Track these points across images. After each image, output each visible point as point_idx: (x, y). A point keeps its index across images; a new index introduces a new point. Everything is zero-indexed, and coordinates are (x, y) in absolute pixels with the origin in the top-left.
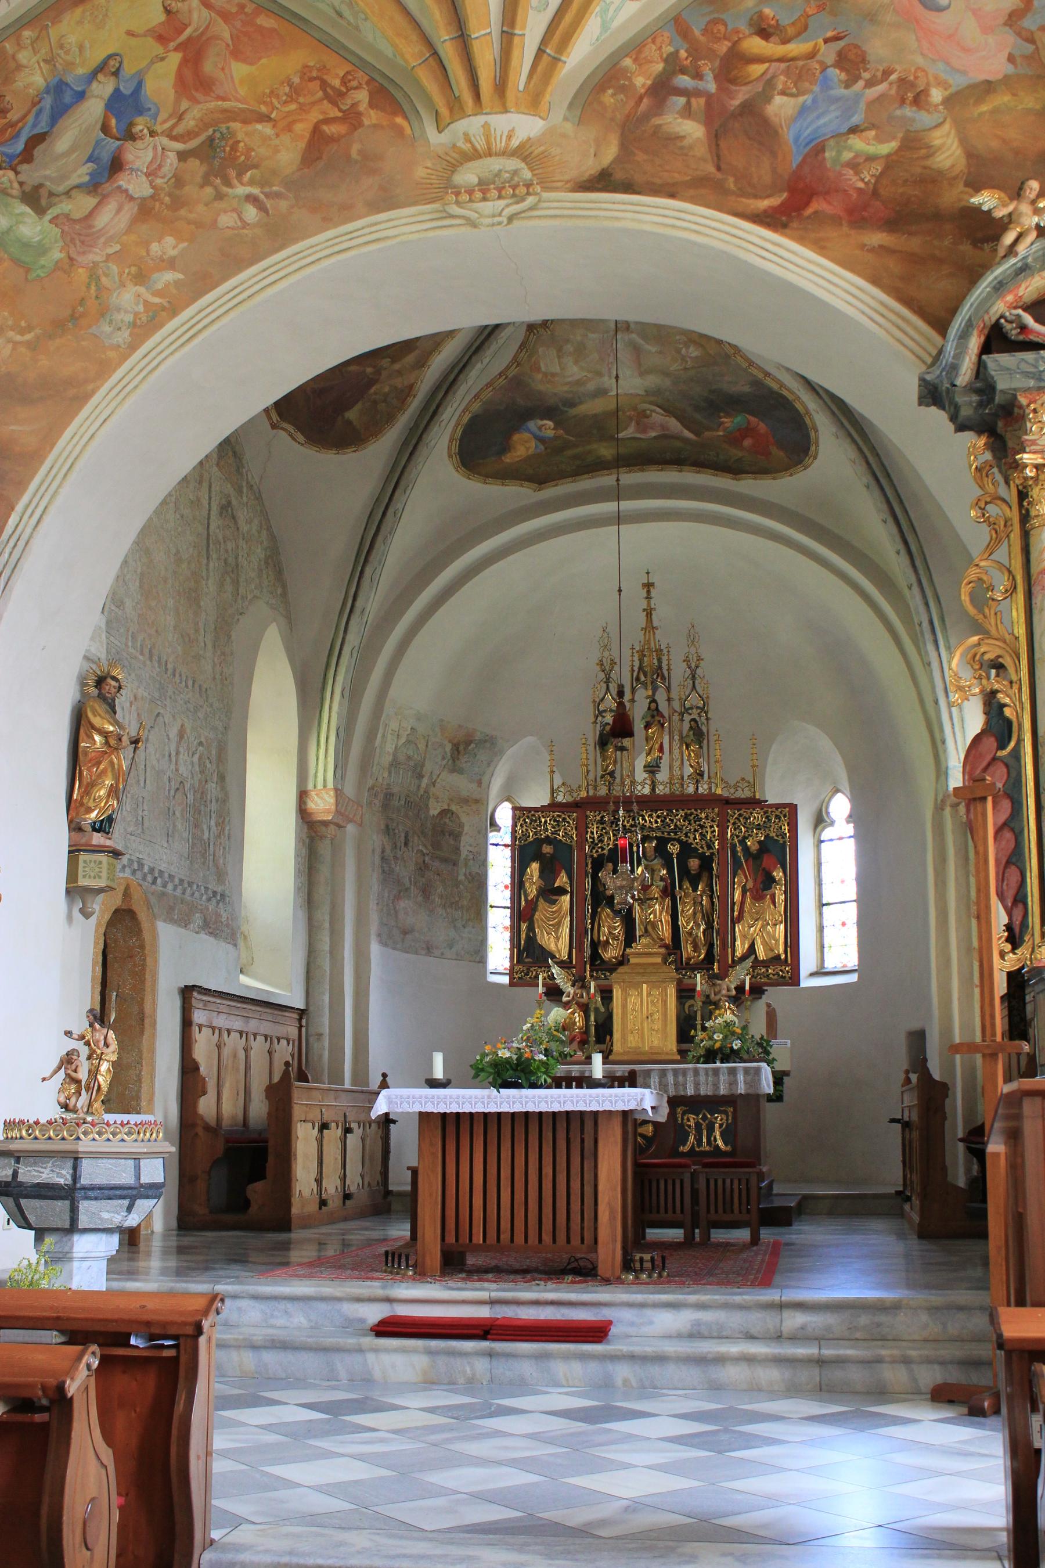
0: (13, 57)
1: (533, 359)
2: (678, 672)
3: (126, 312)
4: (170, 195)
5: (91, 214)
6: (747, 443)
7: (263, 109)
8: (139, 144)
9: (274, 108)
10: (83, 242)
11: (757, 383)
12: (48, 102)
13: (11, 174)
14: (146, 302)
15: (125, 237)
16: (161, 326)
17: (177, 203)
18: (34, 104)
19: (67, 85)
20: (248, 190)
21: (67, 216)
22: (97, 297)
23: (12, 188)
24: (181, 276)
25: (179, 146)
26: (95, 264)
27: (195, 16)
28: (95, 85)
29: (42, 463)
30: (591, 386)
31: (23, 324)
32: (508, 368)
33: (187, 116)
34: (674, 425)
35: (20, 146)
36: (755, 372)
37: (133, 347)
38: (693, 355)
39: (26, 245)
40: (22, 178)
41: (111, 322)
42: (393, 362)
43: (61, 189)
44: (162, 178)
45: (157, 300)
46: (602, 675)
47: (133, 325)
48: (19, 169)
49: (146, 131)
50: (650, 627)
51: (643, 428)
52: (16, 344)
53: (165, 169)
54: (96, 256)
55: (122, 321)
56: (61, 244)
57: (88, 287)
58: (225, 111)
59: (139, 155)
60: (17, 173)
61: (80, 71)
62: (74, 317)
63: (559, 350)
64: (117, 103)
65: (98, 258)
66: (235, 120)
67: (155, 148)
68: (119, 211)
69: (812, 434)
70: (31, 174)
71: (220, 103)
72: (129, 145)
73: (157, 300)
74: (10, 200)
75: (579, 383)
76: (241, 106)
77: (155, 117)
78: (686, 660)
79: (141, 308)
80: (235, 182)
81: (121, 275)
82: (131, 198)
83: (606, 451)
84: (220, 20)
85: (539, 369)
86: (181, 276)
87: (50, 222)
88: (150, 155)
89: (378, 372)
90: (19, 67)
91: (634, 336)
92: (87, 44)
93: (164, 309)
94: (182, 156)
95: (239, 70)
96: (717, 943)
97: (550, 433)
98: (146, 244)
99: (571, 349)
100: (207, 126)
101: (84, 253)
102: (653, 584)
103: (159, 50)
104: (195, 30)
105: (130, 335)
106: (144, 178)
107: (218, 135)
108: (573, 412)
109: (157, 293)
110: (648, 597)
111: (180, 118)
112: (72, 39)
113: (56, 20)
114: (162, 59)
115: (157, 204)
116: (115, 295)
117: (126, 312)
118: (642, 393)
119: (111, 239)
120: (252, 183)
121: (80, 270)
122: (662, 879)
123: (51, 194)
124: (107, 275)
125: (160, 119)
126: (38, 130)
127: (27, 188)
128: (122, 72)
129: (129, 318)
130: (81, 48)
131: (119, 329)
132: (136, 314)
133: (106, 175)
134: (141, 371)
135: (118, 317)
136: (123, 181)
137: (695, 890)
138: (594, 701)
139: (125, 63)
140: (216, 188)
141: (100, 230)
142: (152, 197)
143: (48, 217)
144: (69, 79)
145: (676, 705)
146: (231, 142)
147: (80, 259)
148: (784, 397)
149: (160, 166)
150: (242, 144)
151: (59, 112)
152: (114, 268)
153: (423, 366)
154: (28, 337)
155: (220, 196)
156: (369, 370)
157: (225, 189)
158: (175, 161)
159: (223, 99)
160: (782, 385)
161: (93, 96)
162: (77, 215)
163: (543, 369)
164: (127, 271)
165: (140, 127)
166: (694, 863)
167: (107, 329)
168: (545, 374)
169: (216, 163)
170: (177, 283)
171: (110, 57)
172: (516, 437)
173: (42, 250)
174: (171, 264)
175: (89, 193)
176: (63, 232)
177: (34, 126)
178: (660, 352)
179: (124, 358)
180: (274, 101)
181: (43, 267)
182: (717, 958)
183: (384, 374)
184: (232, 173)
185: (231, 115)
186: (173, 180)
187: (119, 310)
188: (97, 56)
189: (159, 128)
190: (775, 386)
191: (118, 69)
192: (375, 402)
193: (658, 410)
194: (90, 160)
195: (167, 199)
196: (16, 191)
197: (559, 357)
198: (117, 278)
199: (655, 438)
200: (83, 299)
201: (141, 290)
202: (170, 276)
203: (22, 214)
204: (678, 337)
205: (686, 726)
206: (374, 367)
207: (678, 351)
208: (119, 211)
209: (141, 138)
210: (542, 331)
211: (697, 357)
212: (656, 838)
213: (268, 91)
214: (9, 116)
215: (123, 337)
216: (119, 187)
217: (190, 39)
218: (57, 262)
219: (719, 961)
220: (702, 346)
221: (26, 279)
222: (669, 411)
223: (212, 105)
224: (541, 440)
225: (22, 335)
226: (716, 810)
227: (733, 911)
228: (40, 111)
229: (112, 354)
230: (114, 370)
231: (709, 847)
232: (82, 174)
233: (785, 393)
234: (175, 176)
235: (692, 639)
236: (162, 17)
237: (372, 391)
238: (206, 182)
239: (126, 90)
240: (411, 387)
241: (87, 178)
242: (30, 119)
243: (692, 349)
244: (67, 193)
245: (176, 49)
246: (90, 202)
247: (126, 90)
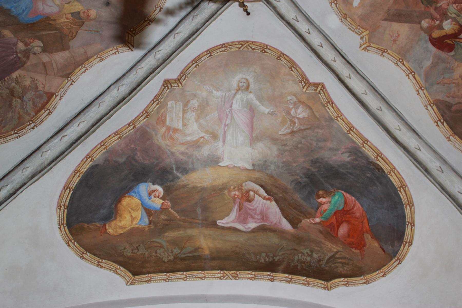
1: (162, 111)
6: (343, 230)
11: (356, 152)
30: (205, 151)
32: (138, 118)
34: (273, 209)
36: (354, 137)
38: (301, 116)
42: (44, 50)
51: (244, 216)
63: (186, 105)
69: (407, 210)
75: (197, 145)
83: (205, 242)
85: (164, 122)
89: (27, 53)
91: (252, 96)
97: (157, 203)
99: (196, 105)
108: (184, 179)
118: (250, 167)
148: (380, 169)
153: (67, 76)
156: (21, 46)
160: (379, 154)
163: (168, 123)
168: (169, 129)
172: (126, 201)
178: (272, 114)
183: (33, 60)
190: (372, 155)
192: (12, 92)
193: (262, 191)
197: (184, 112)
199: (254, 231)
204: (289, 98)
206: (26, 44)
207: (288, 113)
210: (175, 85)
211: (304, 118)
220: (310, 108)
224: (148, 211)
233: (382, 164)
237: (15, 75)
240: (50, 96)
243: (300, 110)
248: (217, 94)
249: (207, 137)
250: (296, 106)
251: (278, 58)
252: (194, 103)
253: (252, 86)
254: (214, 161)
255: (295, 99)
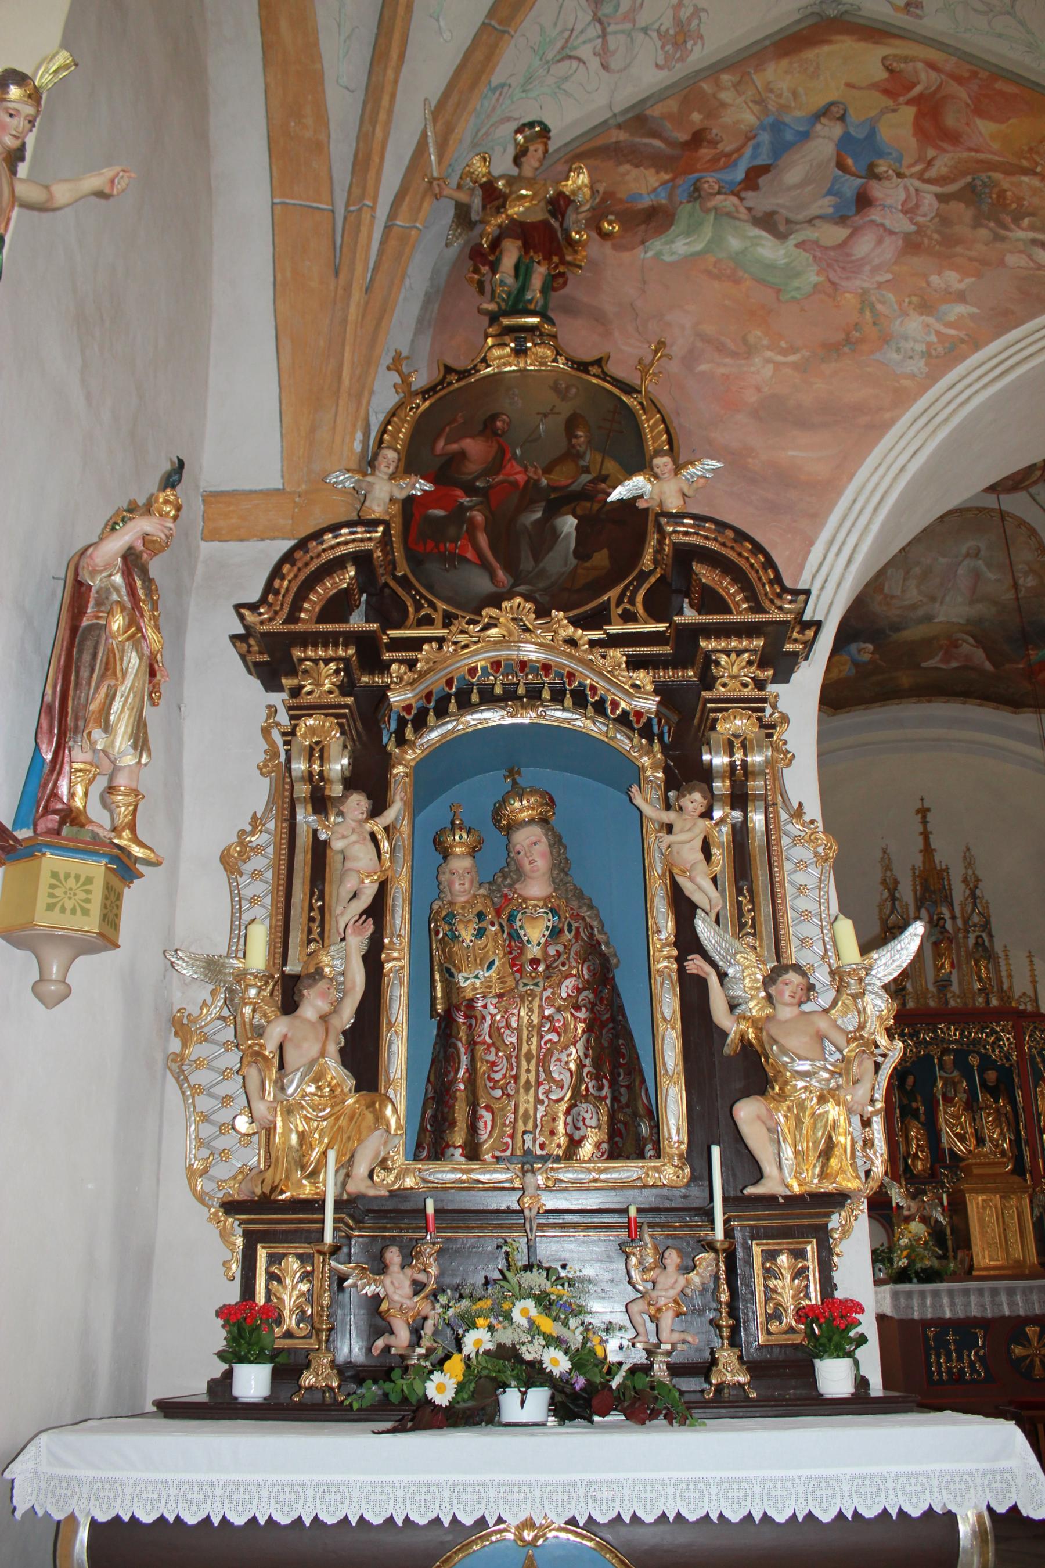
0: (714, 95)
2: (959, 892)
3: (915, 341)
4: (938, 232)
5: (845, 243)
7: (1025, 163)
8: (886, 183)
9: (1037, 164)
10: (843, 268)
12: (765, 137)
13: (735, 200)
14: (938, 333)
15: (896, 268)
16: (964, 358)
17: (950, 241)
18: (749, 139)
19: (785, 124)
20: (1031, 235)
21: (816, 242)
22: (875, 323)
23: (737, 211)
24: (975, 310)
25: (937, 189)
26: (865, 292)
27: (923, 76)
28: (818, 127)
29: (840, 494)
31: (783, 344)
33: (938, 163)
35: (740, 174)
37: (933, 378)
39: (771, 267)
40: (749, 203)
41: (898, 350)
43: (800, 217)
44: (924, 216)
45: (952, 332)
46: (886, 893)
47: (927, 354)
48: (743, 194)
49: (890, 172)
50: (928, 850)
51: (948, 657)
52: (777, 365)
53: (925, 208)
54: (864, 281)
55: (913, 350)
56: (815, 268)
57: (861, 311)
58: (981, 161)
59: (890, 194)
60: (741, 199)
61: (798, 114)
62: (848, 340)
63: (907, 573)
64: (845, 143)
65: (866, 285)
66: (995, 171)
67: (906, 188)
68: (880, 241)
70: (760, 201)
71: (973, 154)
72: (874, 184)
73: (952, 332)
74: (737, 223)
75: (914, 607)
76: (997, 158)
77: (899, 160)
78: (965, 881)
79: (934, 338)
80: (1012, 226)
81: (900, 303)
82: (891, 233)
83: (905, 680)
84: (952, 82)
86: (975, 310)
87: (797, 246)
88: (902, 196)
90: (723, 105)
92: (801, 90)
93: (962, 341)
94: (941, 198)
95: (985, 127)
96: (1027, 1154)
98: (925, 276)
100: (964, 174)
101: (848, 279)
102: (928, 810)
103: (890, 103)
104: (926, 88)
105: (926, 364)
106: (901, 215)
107: (979, 183)
108: (895, 636)
109: (949, 325)
110: (924, 822)
111: (930, 163)
112: (784, 85)
113: (759, 67)
114: (894, 111)
115: (926, 241)
116: (898, 322)
117: (915, 341)
118: (961, 621)
119: (875, 270)
120: (1032, 228)
121: (847, 295)
122: (965, 1091)
123: (788, 221)
124: (883, 303)
125: (905, 163)
126: (759, 162)
127: (759, 215)
128: (848, 119)
129: (921, 347)
130: (795, 94)
131: (911, 358)
132: (929, 344)
133: (854, 209)
134: (949, 403)
135: (909, 345)
136: (875, 215)
137: (997, 1102)
138: (881, 918)
139: (851, 112)
140: (991, 230)
141: (862, 259)
142: (917, 232)
143: (792, 241)
144: (787, 119)
145: (960, 922)
146: (996, 190)
147: (844, 283)
149: (917, 206)
150: (1009, 193)
151: (781, 148)
152: (891, 297)
154: (792, 358)
155: (998, 238)
157: (1003, 232)
158: (936, 204)
159: (977, 151)
161: (818, 137)
162: (829, 243)
163: (886, 590)
164: (907, 300)
165: (884, 169)
166: (992, 1076)
167: (894, 356)
169: (985, 208)
170: (972, 316)
171: (832, 104)
173: (791, 272)
174: (961, 297)
175: (836, 224)
176: (814, 257)
177: (754, 157)
179: (924, 389)
180: (1035, 157)
181: (798, 289)
182: (1028, 1168)
184: (1008, 219)
185: (992, 166)
186: (937, 220)
187: (906, 338)
188: (819, 102)
189: (907, 172)
191: (844, 115)
193: (971, 640)
194: (830, 193)
195: (936, 236)
196: (743, 214)
197: (905, 580)
198: (896, 307)
199: (955, 669)
200: (857, 324)
201: (930, 320)
202: (960, 309)
203: (756, 237)
205: (971, 941)
208: (880, 241)
209: (888, 178)
212: (954, 1050)
213: (1025, 148)
214: (720, 146)
215: (917, 366)
216: (873, 221)
217: (921, 96)
218: (816, 286)
219: (1031, 1172)
221: (778, 300)
222: (979, 642)
223: (965, 155)
224: (856, 664)
225: (785, 356)
226: (1011, 1023)
227: (1039, 1121)
228: (757, 147)
229: (906, 383)
230: (915, 400)
231: (1008, 1060)
232: (825, 205)
234: (937, 215)
235: (969, 861)
236: (885, 75)
238: (976, 224)
239: (859, 134)
241: (831, 210)
242: (748, 152)
243: (1030, 578)
244: (810, 221)
245: (908, 103)
246: (840, 233)
247: (859, 134)
248: (942, 560)
249: (925, 600)
250: (1026, 574)
251: (1019, 526)
252: (917, 570)
253: (982, 553)
254: (929, 618)
255: (1026, 568)
